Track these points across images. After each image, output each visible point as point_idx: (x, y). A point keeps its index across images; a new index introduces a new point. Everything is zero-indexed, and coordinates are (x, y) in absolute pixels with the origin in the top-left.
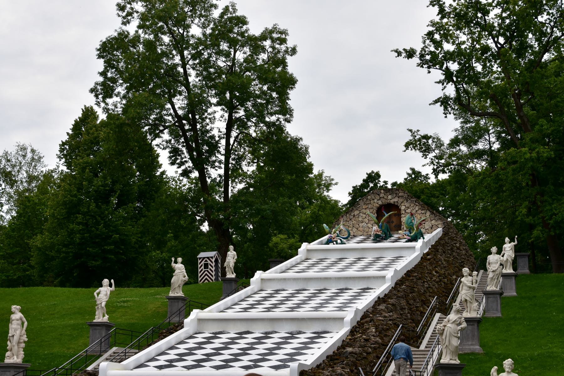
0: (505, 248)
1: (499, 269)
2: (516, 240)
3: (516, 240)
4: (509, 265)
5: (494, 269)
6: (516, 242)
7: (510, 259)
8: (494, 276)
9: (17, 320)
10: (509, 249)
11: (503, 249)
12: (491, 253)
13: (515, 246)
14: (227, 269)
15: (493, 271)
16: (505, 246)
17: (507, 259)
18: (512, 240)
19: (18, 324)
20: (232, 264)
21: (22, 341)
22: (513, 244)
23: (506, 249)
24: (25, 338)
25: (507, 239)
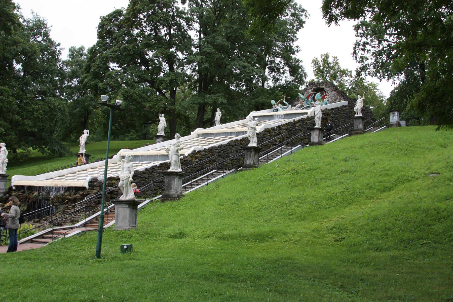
2: (364, 96)
3: (364, 96)
6: (364, 98)
7: (359, 108)
9: (3, 151)
14: (216, 122)
19: (3, 153)
21: (5, 162)
24: (7, 161)
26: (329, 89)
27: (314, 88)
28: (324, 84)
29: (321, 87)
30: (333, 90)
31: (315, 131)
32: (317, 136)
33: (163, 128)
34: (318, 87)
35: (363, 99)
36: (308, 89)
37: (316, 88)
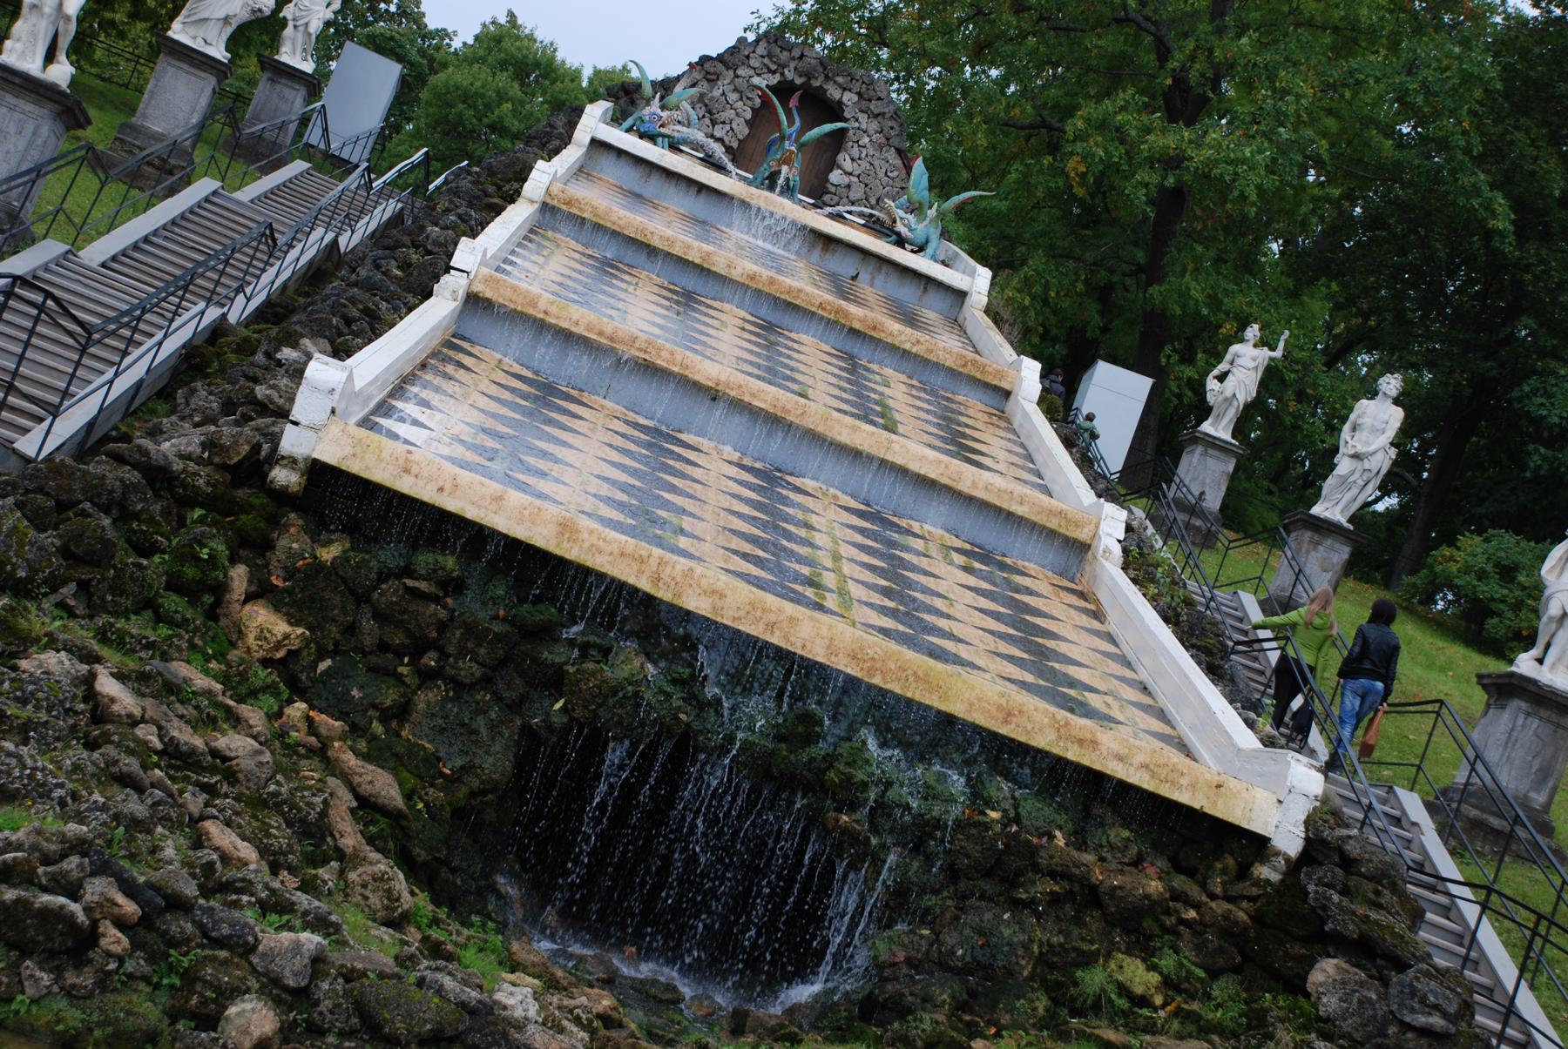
0: (1237, 355)
1: (1380, 456)
2: (1281, 345)
3: (1281, 345)
4: (1231, 414)
5: (1361, 449)
6: (1278, 353)
8: (1353, 472)
10: (1253, 365)
11: (1228, 357)
12: (1373, 394)
13: (1272, 359)
14: (289, 31)
15: (1356, 456)
16: (1235, 348)
17: (1234, 395)
18: (1265, 342)
20: (316, 26)
22: (1265, 353)
23: (1238, 361)
25: (1253, 332)
26: (873, 126)
27: (789, 75)
28: (856, 86)
29: (834, 93)
30: (895, 142)
31: (1329, 542)
32: (1329, 576)
33: (245, 16)
34: (816, 83)
35: (1273, 354)
36: (752, 62)
37: (798, 81)
